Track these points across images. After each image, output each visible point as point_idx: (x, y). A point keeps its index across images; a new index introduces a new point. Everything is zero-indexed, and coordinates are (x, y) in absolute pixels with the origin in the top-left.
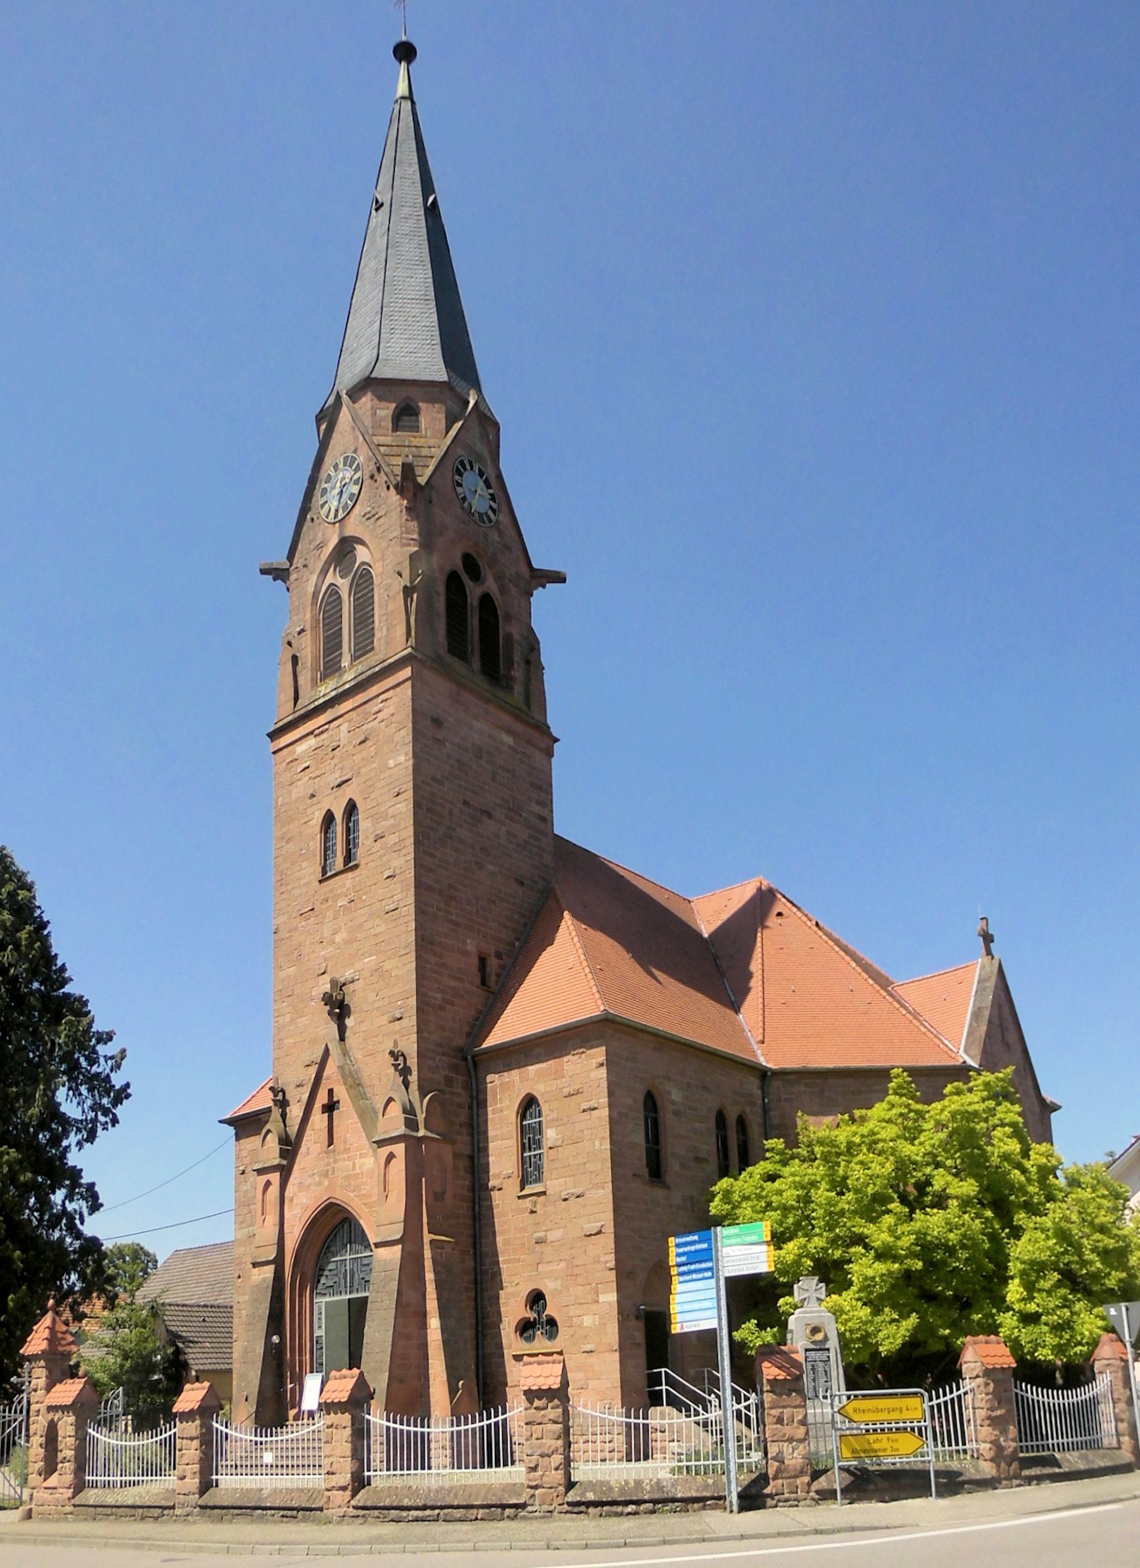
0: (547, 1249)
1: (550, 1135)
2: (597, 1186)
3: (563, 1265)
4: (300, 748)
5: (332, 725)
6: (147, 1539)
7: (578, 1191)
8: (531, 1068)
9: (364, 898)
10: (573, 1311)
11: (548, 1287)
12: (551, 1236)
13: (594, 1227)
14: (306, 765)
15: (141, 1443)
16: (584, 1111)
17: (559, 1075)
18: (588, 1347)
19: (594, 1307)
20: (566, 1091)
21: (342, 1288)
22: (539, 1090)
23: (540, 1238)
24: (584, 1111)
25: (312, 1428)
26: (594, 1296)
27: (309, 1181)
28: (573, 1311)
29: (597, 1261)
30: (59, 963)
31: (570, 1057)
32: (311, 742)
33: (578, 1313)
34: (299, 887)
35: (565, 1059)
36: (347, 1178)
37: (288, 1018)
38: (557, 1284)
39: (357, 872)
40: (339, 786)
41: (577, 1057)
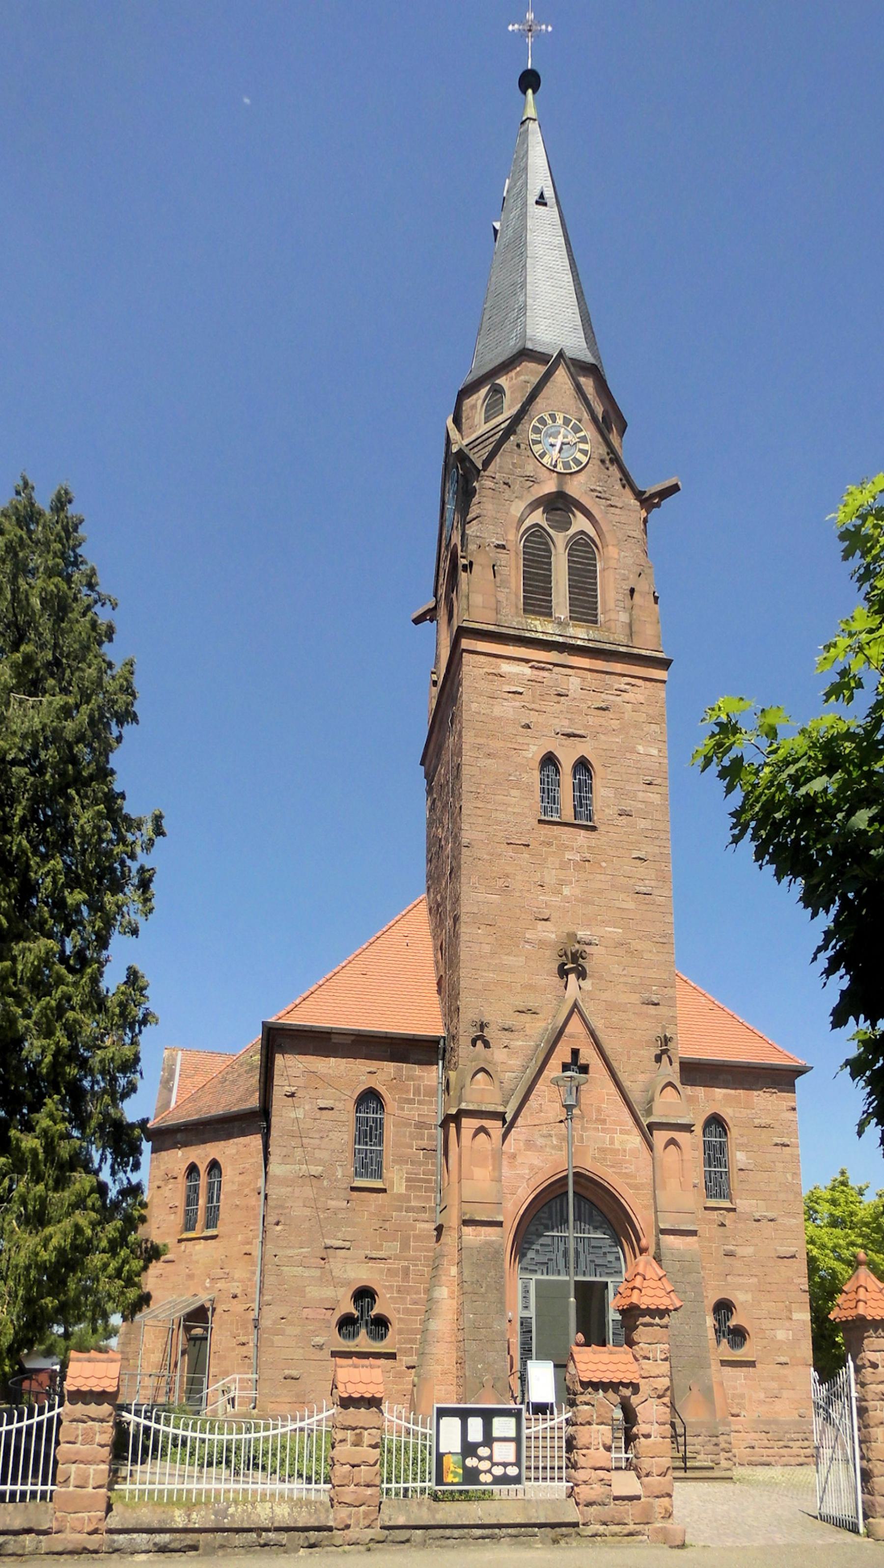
0: (737, 1263)
1: (739, 1157)
2: (789, 1214)
3: (754, 1280)
4: (506, 667)
5: (556, 669)
6: (630, 1534)
7: (770, 1215)
8: (716, 1090)
9: (604, 864)
10: (766, 1324)
11: (739, 1298)
12: (740, 1251)
13: (785, 1250)
14: (521, 690)
15: (226, 1437)
16: (776, 1145)
17: (749, 1106)
18: (783, 1359)
19: (787, 1324)
20: (757, 1122)
21: (561, 1265)
22: (727, 1113)
23: (732, 1251)
24: (776, 1145)
25: (549, 1424)
26: (788, 1313)
27: (540, 1141)
28: (766, 1324)
29: (790, 1281)
30: (748, 846)
31: (760, 1093)
32: (525, 670)
33: (770, 1326)
34: (505, 812)
35: (756, 1093)
36: (602, 1150)
37: (487, 949)
38: (748, 1297)
39: (593, 834)
40: (569, 735)
41: (768, 1095)
